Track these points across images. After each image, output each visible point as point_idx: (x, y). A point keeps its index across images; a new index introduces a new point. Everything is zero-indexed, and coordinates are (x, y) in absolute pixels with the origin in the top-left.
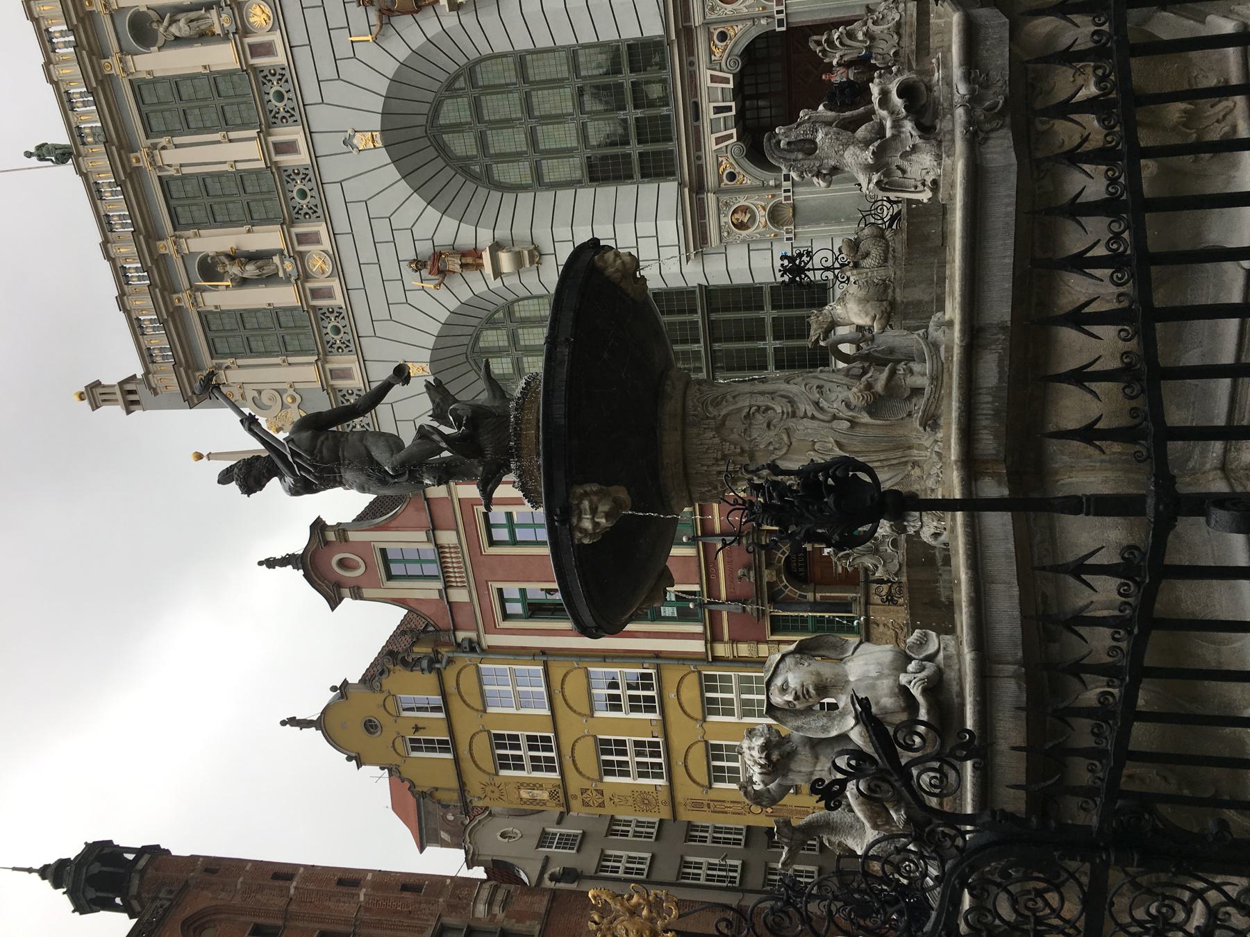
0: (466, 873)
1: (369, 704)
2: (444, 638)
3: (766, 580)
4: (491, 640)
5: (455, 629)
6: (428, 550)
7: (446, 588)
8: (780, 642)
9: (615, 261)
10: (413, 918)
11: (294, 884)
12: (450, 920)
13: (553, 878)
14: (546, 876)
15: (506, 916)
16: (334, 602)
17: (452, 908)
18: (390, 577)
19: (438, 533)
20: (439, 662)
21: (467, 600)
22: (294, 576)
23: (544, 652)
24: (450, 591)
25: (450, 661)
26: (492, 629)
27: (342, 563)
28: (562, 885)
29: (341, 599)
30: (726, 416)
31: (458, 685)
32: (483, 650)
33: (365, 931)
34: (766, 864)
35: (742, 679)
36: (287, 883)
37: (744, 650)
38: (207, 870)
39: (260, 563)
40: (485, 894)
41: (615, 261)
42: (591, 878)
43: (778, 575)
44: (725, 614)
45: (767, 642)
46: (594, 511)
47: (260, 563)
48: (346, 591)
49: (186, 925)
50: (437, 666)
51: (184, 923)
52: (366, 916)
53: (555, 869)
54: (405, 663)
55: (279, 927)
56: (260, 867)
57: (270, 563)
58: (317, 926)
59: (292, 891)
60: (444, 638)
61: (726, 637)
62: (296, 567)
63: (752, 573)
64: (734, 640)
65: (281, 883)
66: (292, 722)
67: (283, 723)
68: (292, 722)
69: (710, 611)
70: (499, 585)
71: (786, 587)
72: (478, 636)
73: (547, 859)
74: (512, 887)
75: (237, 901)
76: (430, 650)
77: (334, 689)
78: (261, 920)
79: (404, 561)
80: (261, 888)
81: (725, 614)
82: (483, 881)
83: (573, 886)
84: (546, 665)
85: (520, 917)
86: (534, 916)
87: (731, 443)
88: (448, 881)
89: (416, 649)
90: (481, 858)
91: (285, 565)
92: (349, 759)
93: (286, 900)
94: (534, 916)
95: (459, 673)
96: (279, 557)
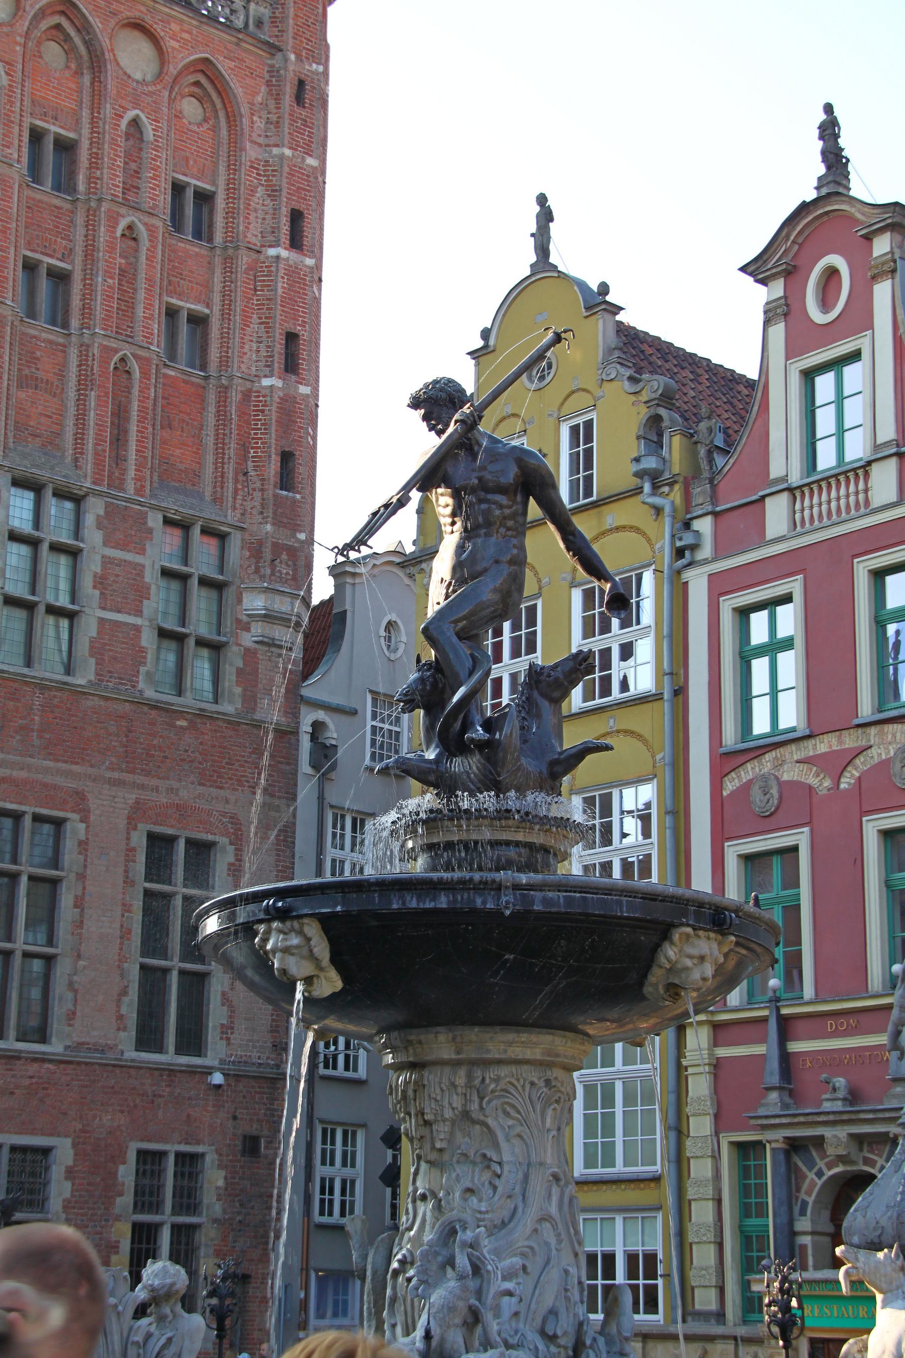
0: (323, 560)
1: (582, 356)
2: (700, 492)
3: (828, 1132)
4: (698, 584)
5: (715, 514)
6: (857, 448)
7: (791, 490)
8: (716, 1157)
9: (690, 957)
10: (236, 481)
11: (284, 253)
12: (235, 543)
13: (318, 727)
14: (321, 715)
15: (247, 650)
16: (756, 269)
17: (255, 550)
18: (809, 375)
19: (893, 463)
20: (655, 487)
21: (770, 534)
22: (803, 181)
23: (680, 692)
24: (785, 497)
25: (658, 510)
26: (720, 586)
27: (832, 273)
28: (305, 743)
29: (763, 282)
30: (484, 1124)
31: (617, 529)
32: (679, 572)
33: (212, 397)
34: (363, 1126)
35: (647, 1081)
36: (285, 238)
37: (699, 1086)
38: (301, 83)
39: (828, 109)
40: (282, 605)
41: (690, 957)
42: (321, 798)
43: (842, 1159)
44: (759, 1049)
45: (717, 1134)
46: (286, 950)
47: (828, 109)
48: (778, 288)
49: (205, 67)
50: (647, 487)
51: (207, 59)
52: (235, 397)
53: (332, 735)
54: (655, 421)
55: (210, 240)
56: (313, 185)
57: (829, 129)
58: (216, 308)
59: (272, 252)
60: (700, 492)
61: (723, 1052)
62: (822, 182)
63: (838, 1106)
64: (717, 1066)
65: (285, 228)
66: (546, 216)
67: (542, 200)
68: (546, 216)
69: (764, 1020)
70: (798, 597)
71: (820, 1174)
72: (706, 562)
73: (353, 713)
74: (297, 654)
75: (251, 153)
76: (676, 470)
77: (604, 289)
78: (220, 203)
79: (840, 399)
80: (273, 193)
81: (759, 1049)
82: (306, 601)
83: (305, 767)
84: (657, 697)
85: (248, 676)
86: (250, 700)
87: (452, 1133)
88: (302, 536)
89: (677, 440)
90: (348, 589)
91: (825, 160)
92: (485, 334)
93: (256, 241)
94: (250, 700)
95: (637, 530)
96: (842, 142)
